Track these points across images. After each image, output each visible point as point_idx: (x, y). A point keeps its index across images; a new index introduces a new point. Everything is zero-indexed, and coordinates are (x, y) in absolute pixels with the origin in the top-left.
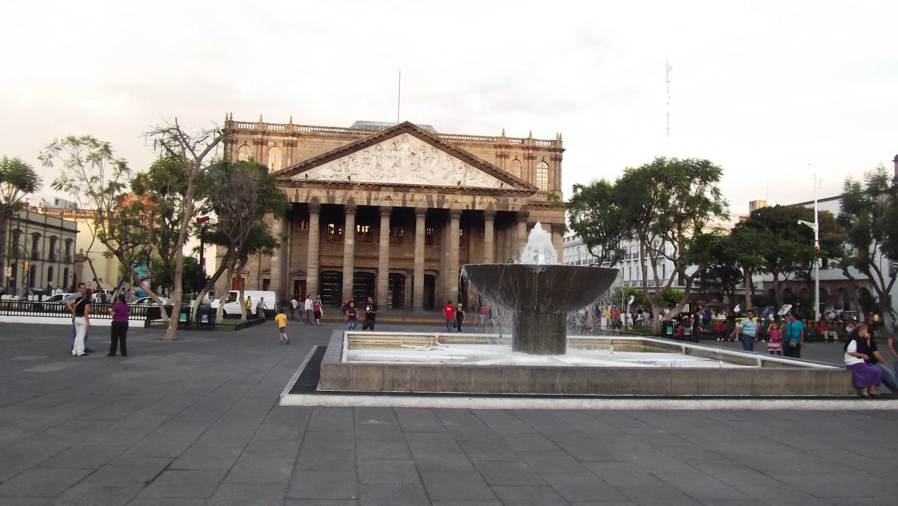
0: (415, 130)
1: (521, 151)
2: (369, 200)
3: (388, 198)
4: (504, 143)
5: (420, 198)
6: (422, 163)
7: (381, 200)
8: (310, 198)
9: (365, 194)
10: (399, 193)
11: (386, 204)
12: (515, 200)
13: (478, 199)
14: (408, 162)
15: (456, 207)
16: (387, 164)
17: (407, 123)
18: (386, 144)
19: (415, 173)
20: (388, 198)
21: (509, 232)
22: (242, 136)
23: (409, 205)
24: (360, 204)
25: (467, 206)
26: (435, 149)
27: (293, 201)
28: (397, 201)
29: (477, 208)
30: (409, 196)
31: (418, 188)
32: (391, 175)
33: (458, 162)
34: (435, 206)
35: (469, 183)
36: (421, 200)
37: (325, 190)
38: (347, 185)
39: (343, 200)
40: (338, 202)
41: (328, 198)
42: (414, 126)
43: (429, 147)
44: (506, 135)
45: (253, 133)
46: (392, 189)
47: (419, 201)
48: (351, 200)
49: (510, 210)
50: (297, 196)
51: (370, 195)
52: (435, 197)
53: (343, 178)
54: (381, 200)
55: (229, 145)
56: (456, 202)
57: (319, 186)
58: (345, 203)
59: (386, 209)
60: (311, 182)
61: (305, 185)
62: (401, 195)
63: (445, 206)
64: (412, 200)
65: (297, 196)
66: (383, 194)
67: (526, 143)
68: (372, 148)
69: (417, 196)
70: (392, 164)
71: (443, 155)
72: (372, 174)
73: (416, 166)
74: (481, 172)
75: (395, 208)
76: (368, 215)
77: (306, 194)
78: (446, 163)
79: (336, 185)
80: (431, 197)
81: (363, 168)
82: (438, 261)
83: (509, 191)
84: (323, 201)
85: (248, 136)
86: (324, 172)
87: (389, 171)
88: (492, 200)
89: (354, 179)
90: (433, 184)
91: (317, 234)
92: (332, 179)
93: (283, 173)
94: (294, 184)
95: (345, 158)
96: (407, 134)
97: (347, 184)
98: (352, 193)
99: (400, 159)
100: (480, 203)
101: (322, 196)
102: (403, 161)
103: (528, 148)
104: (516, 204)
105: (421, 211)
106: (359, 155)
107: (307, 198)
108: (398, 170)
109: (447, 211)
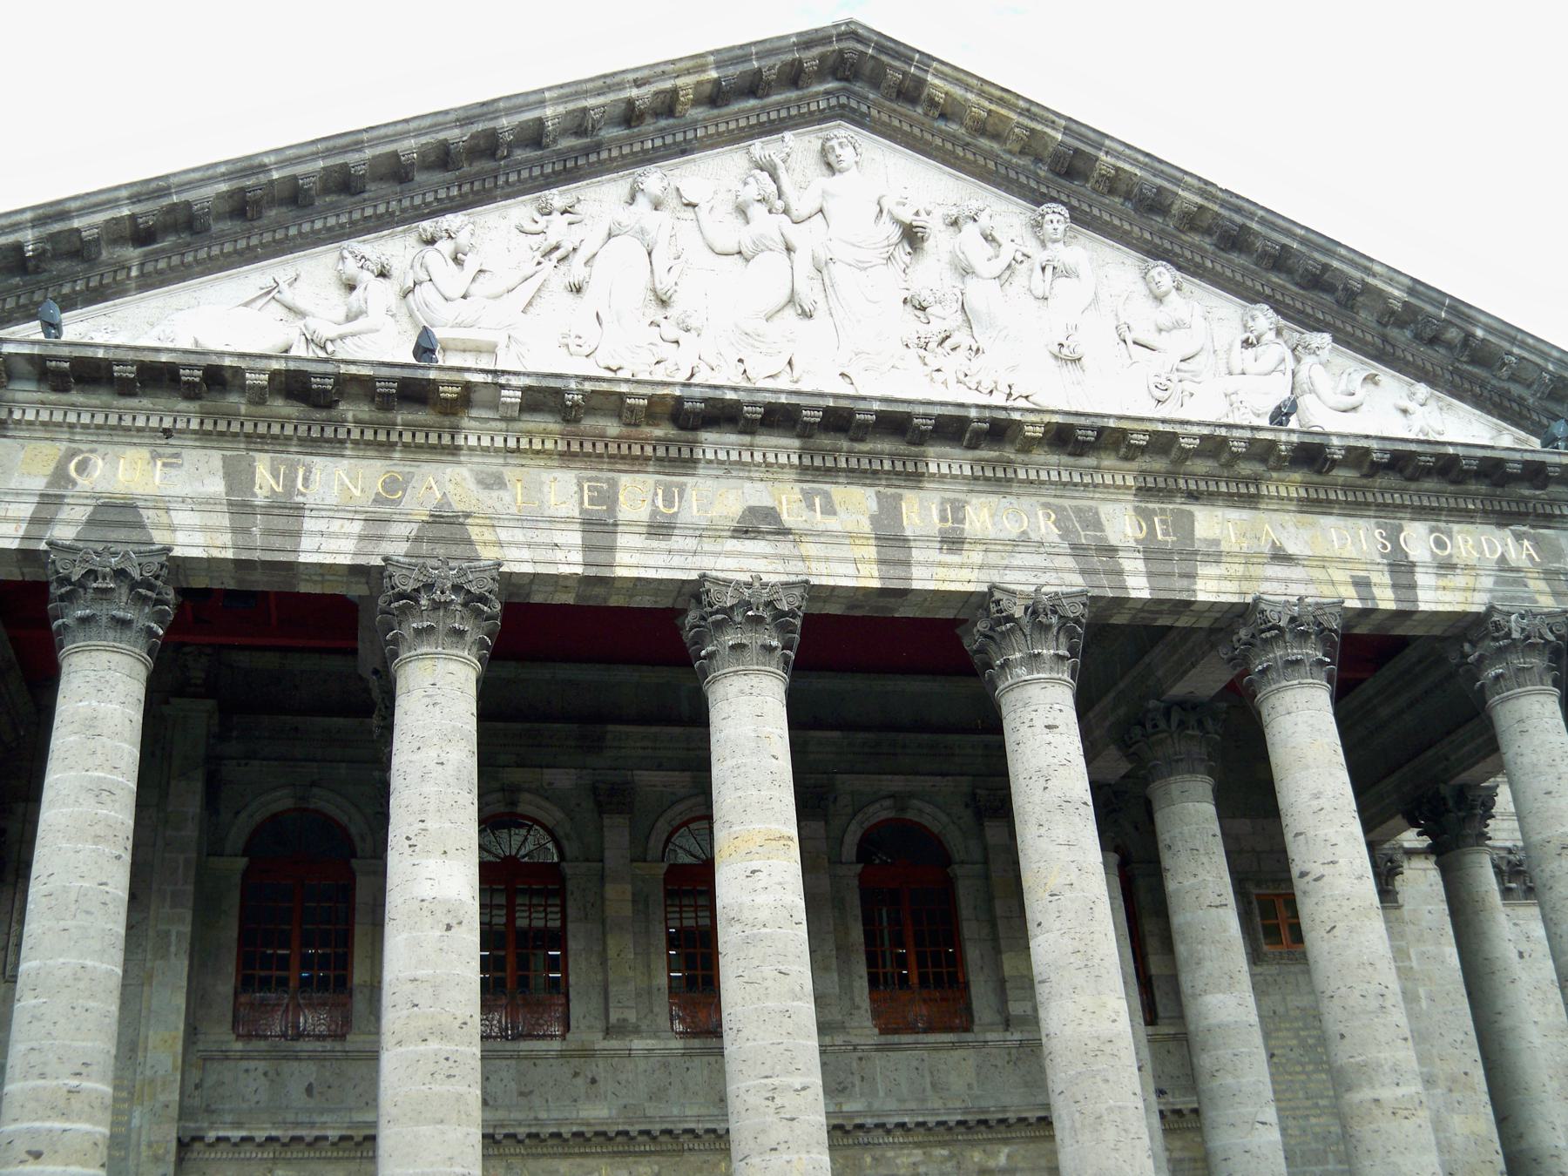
0: (910, 93)
2: (599, 528)
3: (758, 524)
5: (1011, 529)
8: (81, 513)
9: (562, 490)
13: (1417, 539)
15: (1280, 589)
17: (852, 32)
23: (936, 574)
24: (520, 562)
25: (1362, 584)
26: (1056, 217)
28: (837, 541)
29: (1436, 597)
30: (920, 512)
34: (1139, 587)
36: (1022, 542)
37: (215, 458)
38: (414, 404)
39: (376, 523)
40: (328, 544)
41: (241, 509)
42: (902, 53)
43: (1005, 214)
46: (782, 448)
51: (609, 499)
52: (1121, 522)
53: (382, 344)
56: (1280, 557)
57: (146, 411)
60: (88, 373)
62: (856, 504)
63: (1212, 587)
64: (953, 542)
66: (714, 496)
68: (601, 198)
69: (985, 515)
74: (1387, 376)
76: (592, 685)
77: (39, 484)
79: (316, 400)
101: (187, 503)
105: (1042, 616)
107: (50, 501)
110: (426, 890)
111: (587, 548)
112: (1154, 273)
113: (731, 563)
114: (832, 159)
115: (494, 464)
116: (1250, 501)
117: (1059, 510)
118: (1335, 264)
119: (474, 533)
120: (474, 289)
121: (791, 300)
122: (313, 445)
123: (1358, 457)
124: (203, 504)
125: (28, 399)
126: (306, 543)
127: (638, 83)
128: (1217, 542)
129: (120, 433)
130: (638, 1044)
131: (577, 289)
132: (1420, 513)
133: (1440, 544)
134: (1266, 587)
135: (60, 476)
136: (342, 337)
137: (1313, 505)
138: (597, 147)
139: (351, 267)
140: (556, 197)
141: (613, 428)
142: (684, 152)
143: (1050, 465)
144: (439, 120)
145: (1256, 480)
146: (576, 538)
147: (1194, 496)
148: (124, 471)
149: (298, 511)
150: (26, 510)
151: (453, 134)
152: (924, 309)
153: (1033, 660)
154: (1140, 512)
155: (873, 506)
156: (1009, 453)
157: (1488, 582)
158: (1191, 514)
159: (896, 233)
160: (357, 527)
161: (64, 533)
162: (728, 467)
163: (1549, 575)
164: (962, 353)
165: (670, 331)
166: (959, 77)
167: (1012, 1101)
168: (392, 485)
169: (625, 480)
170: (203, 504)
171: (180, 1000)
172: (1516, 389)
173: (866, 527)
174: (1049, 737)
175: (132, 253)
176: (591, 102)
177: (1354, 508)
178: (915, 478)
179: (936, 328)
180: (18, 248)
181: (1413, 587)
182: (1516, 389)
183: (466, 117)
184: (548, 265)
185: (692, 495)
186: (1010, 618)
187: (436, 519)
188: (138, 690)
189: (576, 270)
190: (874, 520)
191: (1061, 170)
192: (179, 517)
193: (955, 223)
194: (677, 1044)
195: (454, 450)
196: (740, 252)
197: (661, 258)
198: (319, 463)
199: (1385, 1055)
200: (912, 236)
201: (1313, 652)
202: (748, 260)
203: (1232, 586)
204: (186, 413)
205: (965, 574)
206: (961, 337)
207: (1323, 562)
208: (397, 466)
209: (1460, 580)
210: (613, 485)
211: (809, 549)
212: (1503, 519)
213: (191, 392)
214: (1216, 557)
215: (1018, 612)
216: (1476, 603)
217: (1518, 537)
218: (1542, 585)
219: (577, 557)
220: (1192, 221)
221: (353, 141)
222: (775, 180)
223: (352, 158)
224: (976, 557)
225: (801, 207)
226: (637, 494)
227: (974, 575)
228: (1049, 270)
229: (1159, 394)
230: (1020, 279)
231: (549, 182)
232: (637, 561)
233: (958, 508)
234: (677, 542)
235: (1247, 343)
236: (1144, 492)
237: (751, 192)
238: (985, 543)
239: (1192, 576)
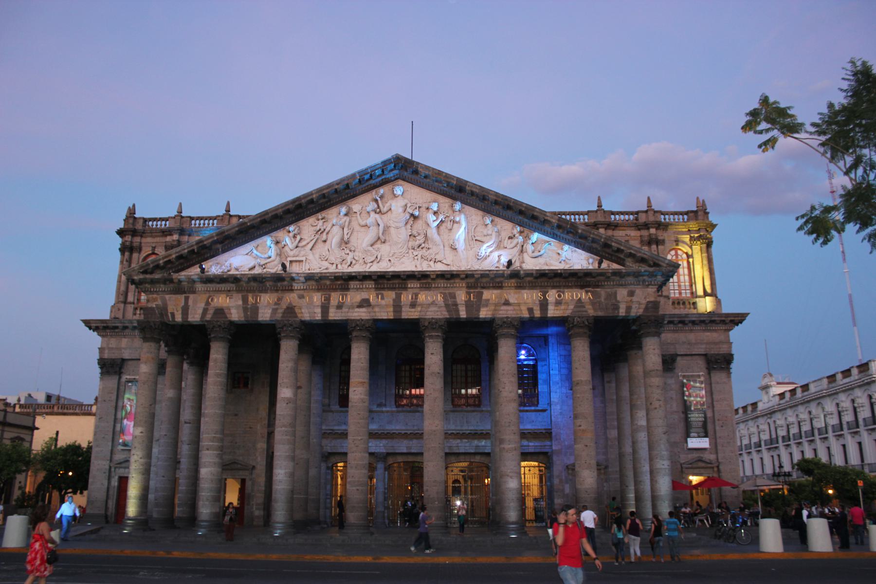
1: (633, 233)
2: (325, 309)
3: (365, 303)
4: (600, 218)
6: (433, 233)
7: (352, 307)
8: (211, 312)
9: (317, 298)
10: (386, 293)
11: (362, 314)
12: (631, 294)
13: (552, 295)
14: (404, 233)
15: (505, 312)
16: (362, 239)
19: (419, 253)
20: (365, 303)
21: (624, 372)
22: (149, 240)
23: (408, 314)
26: (458, 206)
27: (179, 318)
28: (382, 306)
29: (552, 312)
30: (406, 297)
31: (423, 278)
32: (369, 259)
33: (506, 227)
34: (463, 314)
35: (531, 264)
36: (433, 303)
37: (240, 296)
38: (280, 282)
39: (275, 311)
40: (265, 315)
41: (245, 310)
43: (445, 201)
44: (606, 207)
45: (165, 232)
46: (371, 284)
47: (429, 305)
48: (290, 310)
49: (622, 312)
50: (185, 311)
51: (328, 299)
52: (461, 296)
54: (352, 307)
55: (127, 254)
56: (507, 303)
58: (279, 316)
59: (360, 325)
60: (209, 280)
61: (199, 286)
62: (390, 295)
63: (484, 313)
64: (413, 305)
65: (185, 311)
66: (354, 296)
67: (643, 218)
70: (371, 235)
71: (475, 215)
72: (332, 259)
73: (420, 239)
75: (376, 321)
76: (325, 344)
77: (203, 305)
78: (480, 229)
80: (453, 296)
81: (313, 250)
82: (485, 435)
83: (616, 273)
84: (236, 315)
85: (158, 239)
86: (240, 260)
87: (366, 251)
88: (583, 295)
89: (295, 269)
90: (454, 268)
91: (223, 380)
92: (252, 272)
93: (157, 267)
94: (179, 289)
95: (280, 234)
96: (401, 182)
97: (277, 279)
98: (291, 298)
99: (387, 229)
100: (558, 303)
101: (233, 307)
102: (392, 230)
103: (646, 226)
104: (631, 301)
105: (433, 324)
106: (308, 226)
107: (205, 311)
108: (384, 249)
109: (489, 323)
110: (283, 395)
111: (322, 312)
113: (356, 314)
115: (301, 292)
116: (500, 287)
117: (444, 294)
118: (535, 214)
119: (297, 310)
120: (300, 245)
121: (379, 238)
122: (261, 292)
123: (529, 274)
124: (237, 307)
125: (199, 286)
126: (260, 315)
127: (338, 184)
128: (488, 300)
129: (219, 291)
130: (384, 409)
132: (554, 287)
133: (559, 296)
134: (501, 312)
135: (208, 303)
137: (520, 287)
138: (330, 201)
140: (320, 216)
141: (328, 282)
143: (441, 283)
144: (287, 204)
145: (501, 282)
146: (318, 310)
147: (484, 288)
148: (220, 301)
149: (257, 309)
150: (200, 311)
151: (291, 206)
153: (431, 337)
154: (469, 294)
155: (394, 296)
156: (430, 281)
157: (571, 307)
158: (482, 293)
159: (408, 216)
160: (270, 311)
161: (208, 317)
162: (357, 289)
163: (593, 303)
164: (424, 250)
165: (348, 251)
166: (427, 168)
167: (486, 427)
168: (279, 299)
169: (333, 294)
170: (237, 307)
171: (267, 399)
172: (595, 245)
173: (392, 302)
174: (432, 356)
175: (219, 246)
176: (325, 192)
177: (532, 286)
178: (406, 288)
179: (418, 243)
180: (193, 250)
181: (547, 309)
182: (595, 245)
183: (293, 201)
184: (317, 236)
185: (349, 297)
187: (288, 308)
188: (226, 351)
189: (324, 236)
190: (394, 300)
191: (459, 191)
192: (234, 311)
193: (428, 209)
194: (395, 409)
195: (292, 290)
198: (263, 295)
199: (507, 437)
201: (513, 331)
203: (490, 313)
204: (233, 286)
205: (416, 313)
207: (519, 305)
208: (280, 294)
209: (563, 307)
210: (330, 296)
211: (377, 309)
212: (582, 287)
213: (233, 283)
214: (487, 306)
215: (426, 324)
216: (568, 313)
217: (587, 292)
218: (590, 307)
219: (320, 315)
220: (496, 203)
221: (266, 213)
223: (267, 217)
224: (419, 309)
225: (384, 210)
226: (335, 298)
227: (416, 313)
230: (444, 225)
231: (318, 212)
232: (334, 315)
233: (417, 295)
234: (345, 310)
235: (510, 238)
236: (468, 287)
237: (369, 209)
238: (422, 305)
239: (479, 311)
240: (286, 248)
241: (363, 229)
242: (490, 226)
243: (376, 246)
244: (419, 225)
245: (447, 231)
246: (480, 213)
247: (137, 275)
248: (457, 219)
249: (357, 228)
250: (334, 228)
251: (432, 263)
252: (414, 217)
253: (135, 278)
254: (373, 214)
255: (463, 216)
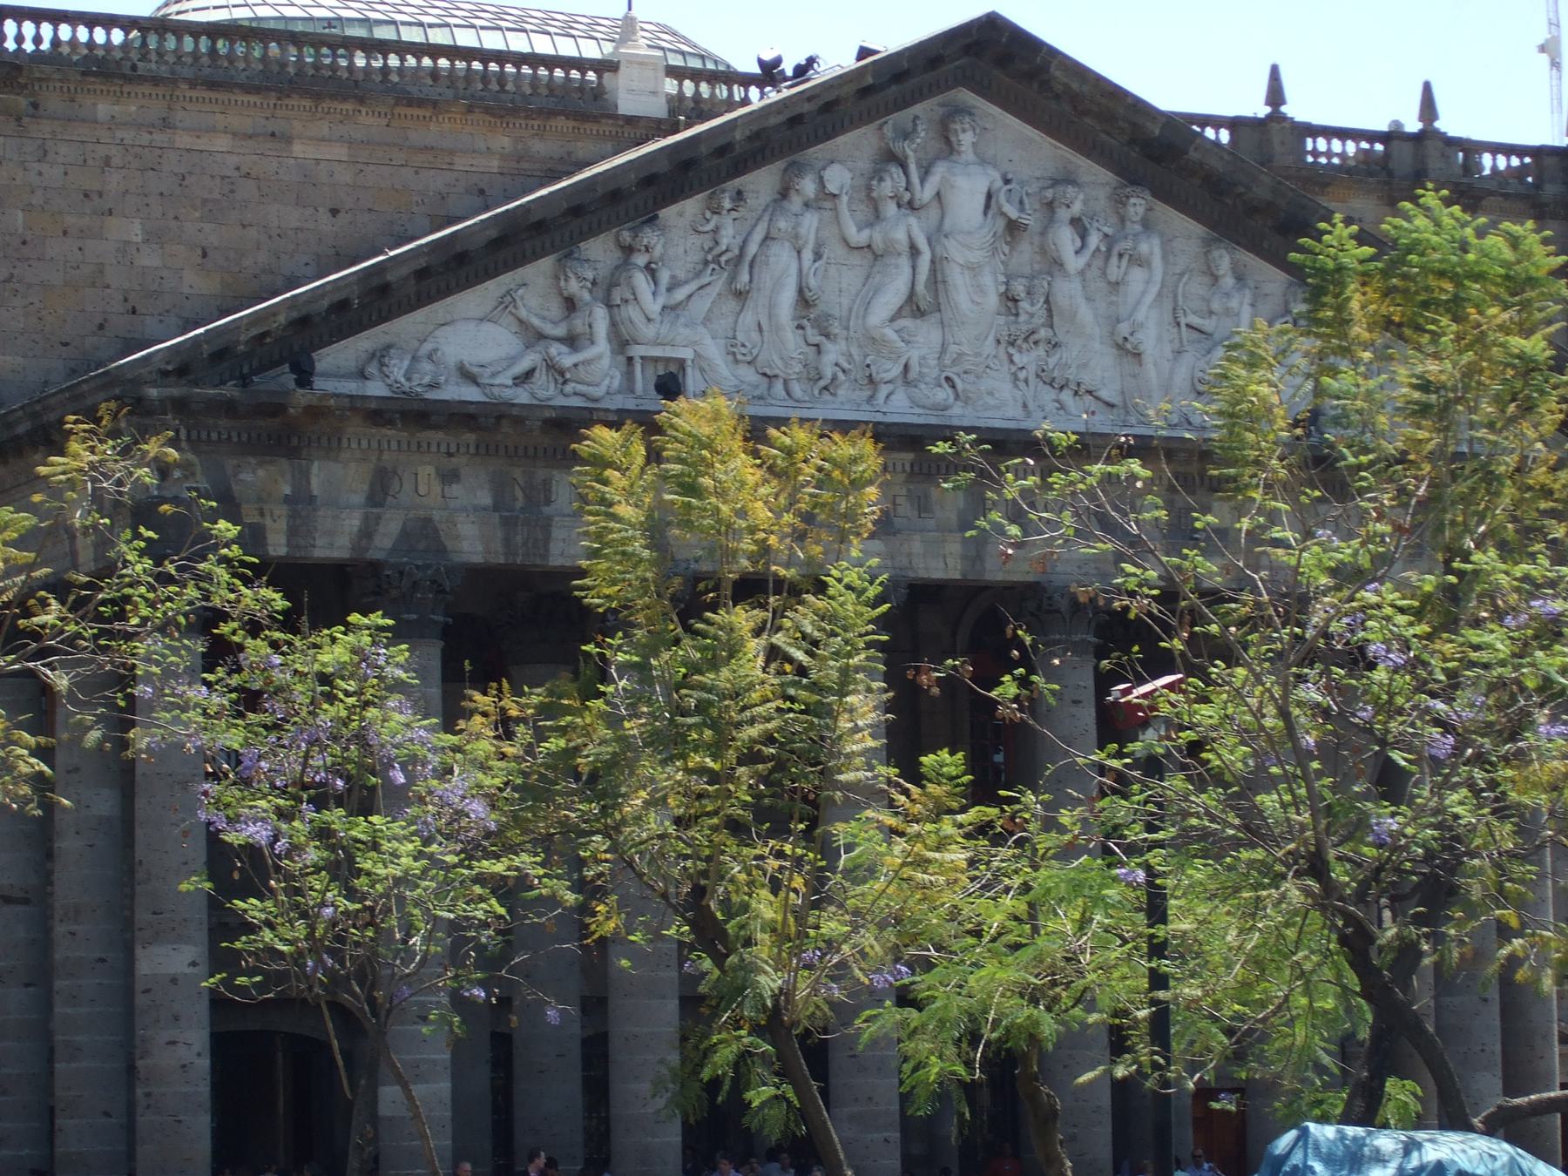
6: (1068, 291)
14: (992, 286)
18: (841, 164)
19: (1027, 359)
84: (472, 542)
87: (873, 341)
96: (966, 96)
112: (1216, 253)
114: (953, 139)
126: (555, 548)
131: (741, 295)
136: (576, 365)
139: (573, 287)
142: (829, 138)
150: (353, 522)
152: (1016, 301)
159: (1001, 224)
164: (1041, 351)
174: (1073, 710)
186: (1058, 611)
196: (869, 246)
197: (808, 255)
200: (1013, 228)
202: (876, 257)
206: (1043, 333)
215: (1063, 605)
222: (906, 173)
225: (926, 194)
228: (1126, 258)
229: (1201, 388)
240: (632, 311)
241: (856, 259)
242: (1228, 281)
243: (902, 323)
244: (1025, 256)
245: (1102, 285)
246: (1197, 229)
247: (154, 384)
248: (1144, 248)
249: (834, 251)
250: (775, 248)
251: (1066, 396)
252: (1013, 228)
253: (153, 392)
254: (890, 209)
255: (1156, 242)
